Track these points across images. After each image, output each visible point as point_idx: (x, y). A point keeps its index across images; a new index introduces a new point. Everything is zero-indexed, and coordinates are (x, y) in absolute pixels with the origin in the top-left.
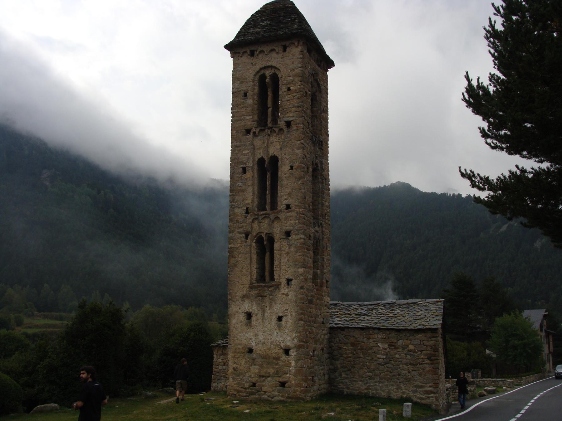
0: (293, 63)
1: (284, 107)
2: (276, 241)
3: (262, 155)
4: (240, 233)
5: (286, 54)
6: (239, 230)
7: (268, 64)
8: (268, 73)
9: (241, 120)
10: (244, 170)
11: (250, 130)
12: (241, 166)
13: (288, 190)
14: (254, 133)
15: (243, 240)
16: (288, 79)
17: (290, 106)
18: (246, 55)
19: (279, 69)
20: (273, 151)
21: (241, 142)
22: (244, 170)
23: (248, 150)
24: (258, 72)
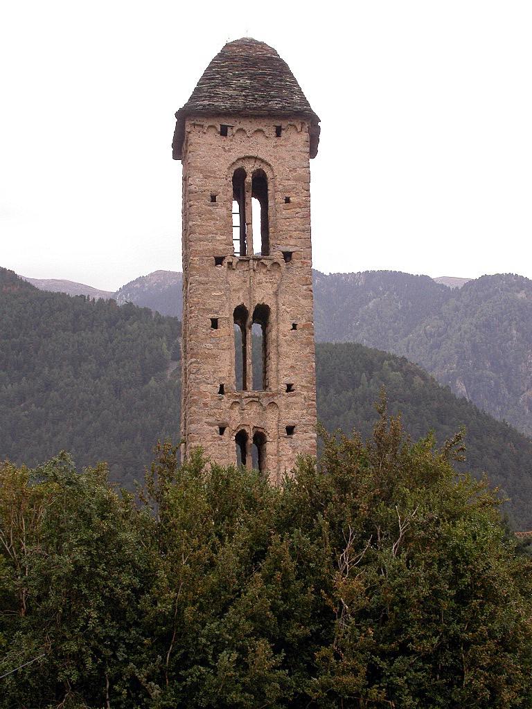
0: (293, 158)
1: (279, 227)
2: (268, 439)
3: (242, 301)
4: (210, 424)
5: (281, 141)
6: (211, 420)
7: (251, 154)
8: (250, 168)
9: (208, 240)
10: (215, 323)
11: (224, 258)
12: (211, 316)
13: (290, 362)
14: (230, 264)
15: (217, 435)
16: (286, 183)
17: (290, 228)
18: (213, 131)
19: (270, 165)
20: (262, 295)
21: (207, 275)
22: (215, 323)
23: (220, 290)
24: (234, 163)
